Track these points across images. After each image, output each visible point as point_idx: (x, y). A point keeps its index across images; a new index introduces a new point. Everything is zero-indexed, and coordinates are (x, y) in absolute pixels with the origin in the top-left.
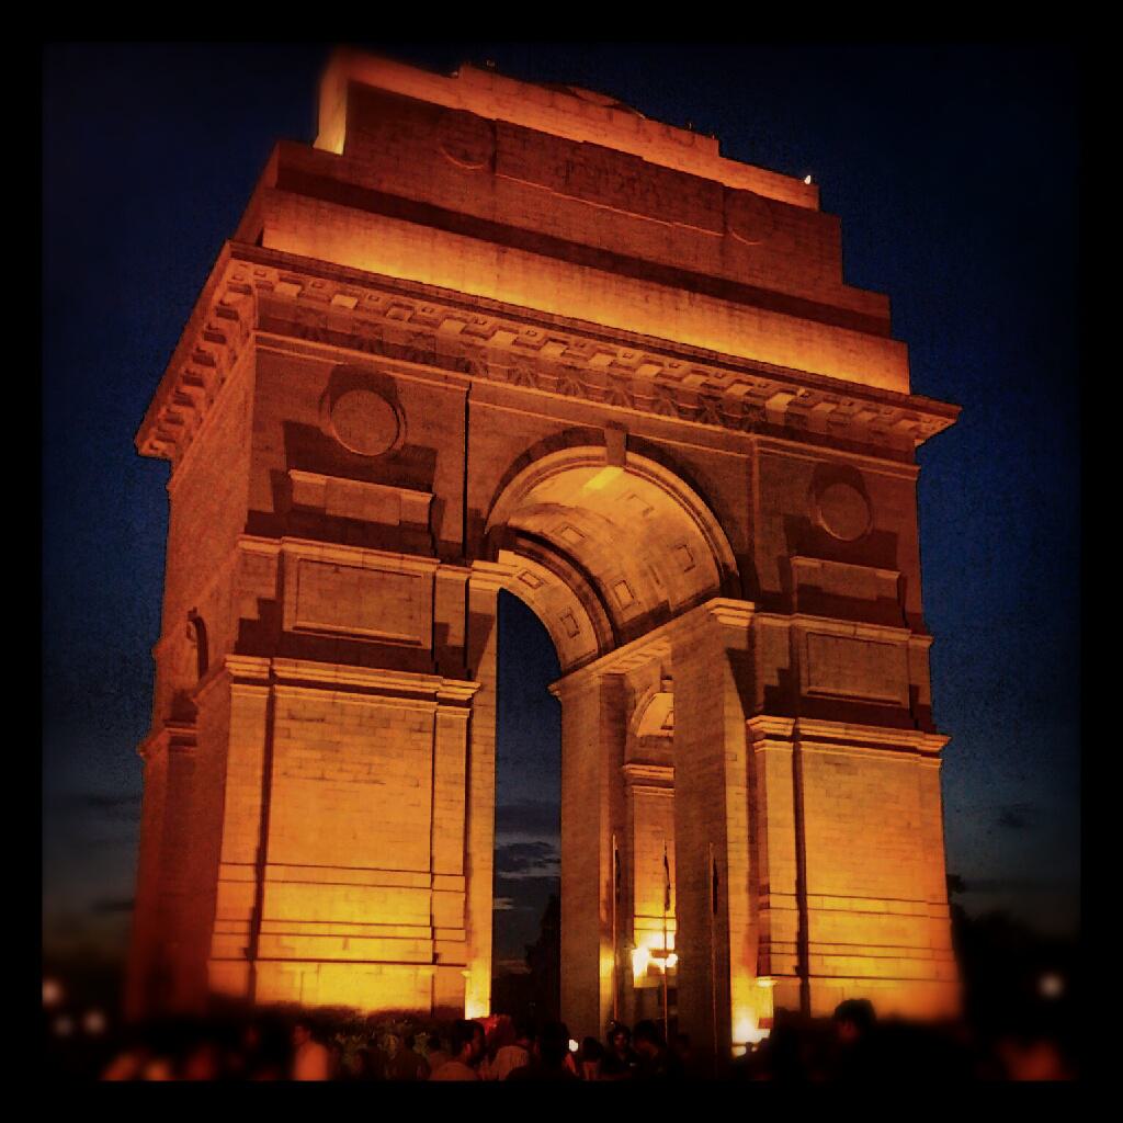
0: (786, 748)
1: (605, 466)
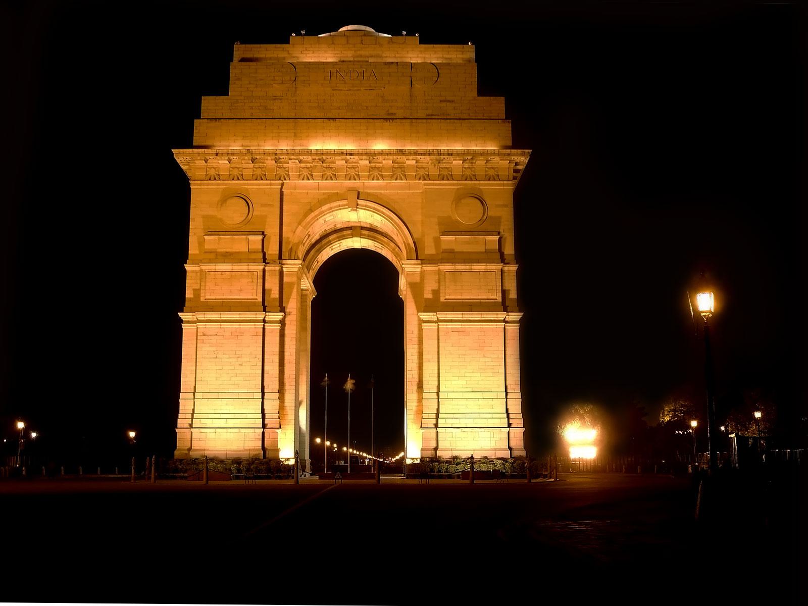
1: (348, 208)
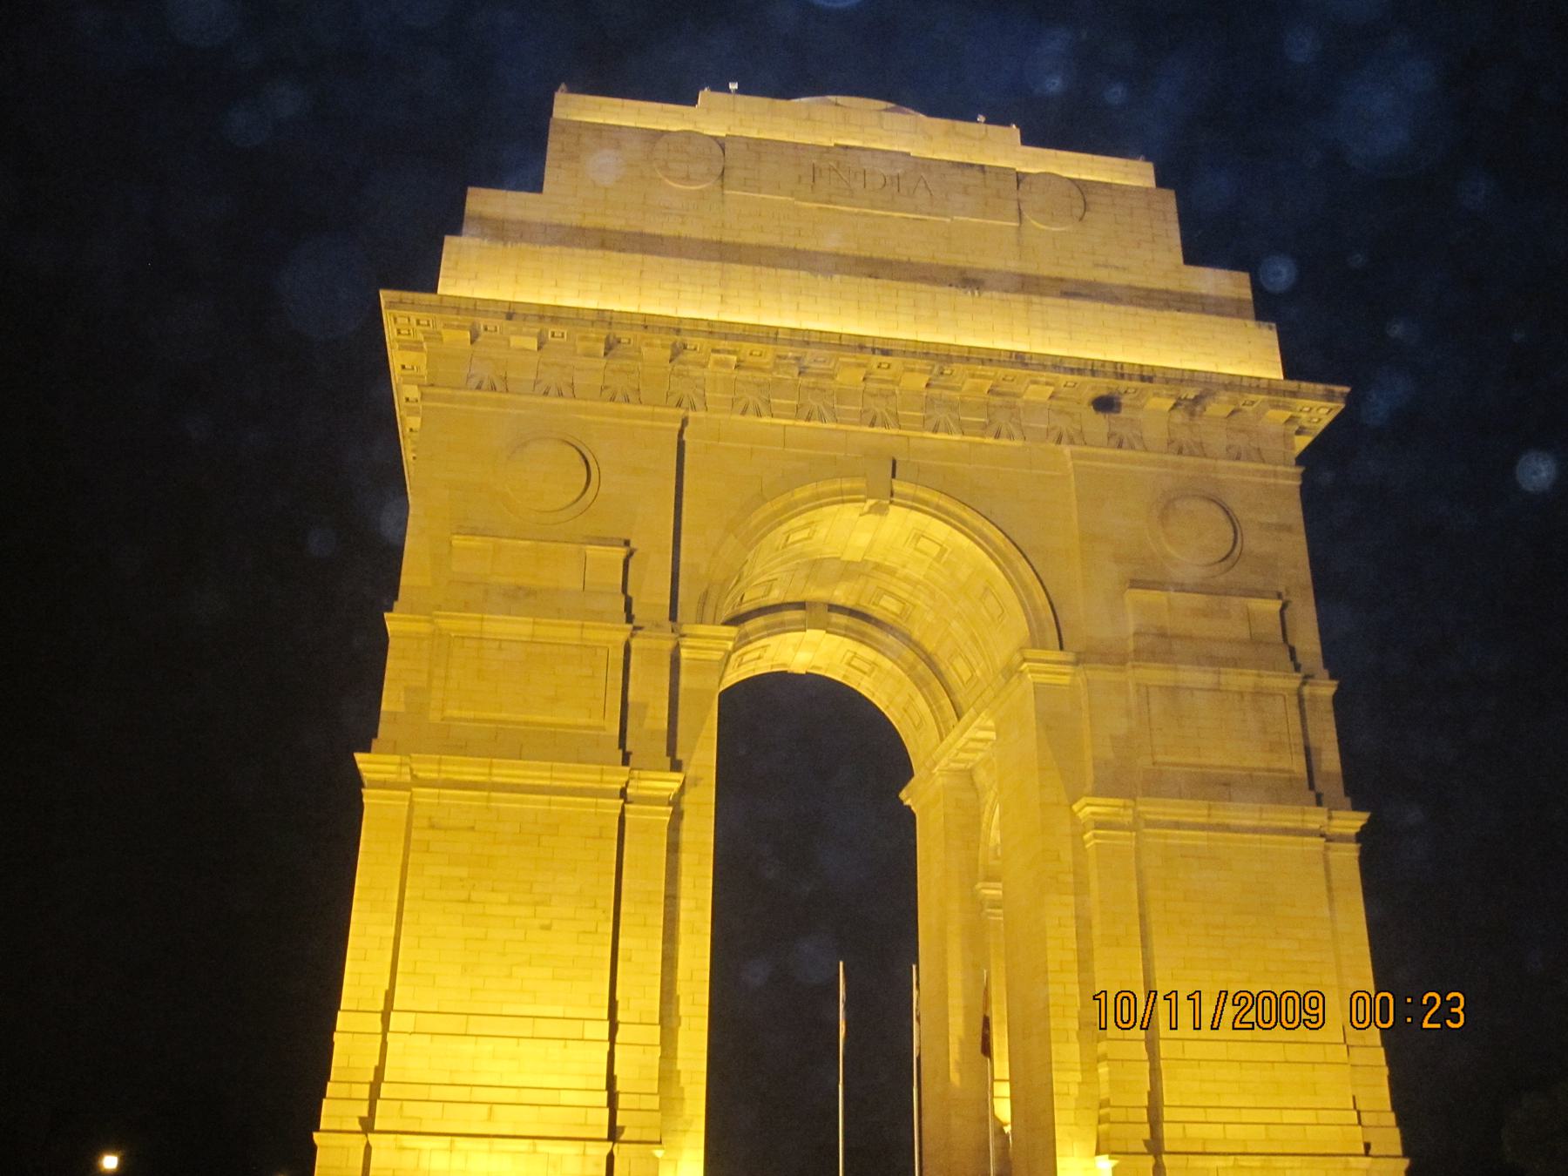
0: (1125, 839)
